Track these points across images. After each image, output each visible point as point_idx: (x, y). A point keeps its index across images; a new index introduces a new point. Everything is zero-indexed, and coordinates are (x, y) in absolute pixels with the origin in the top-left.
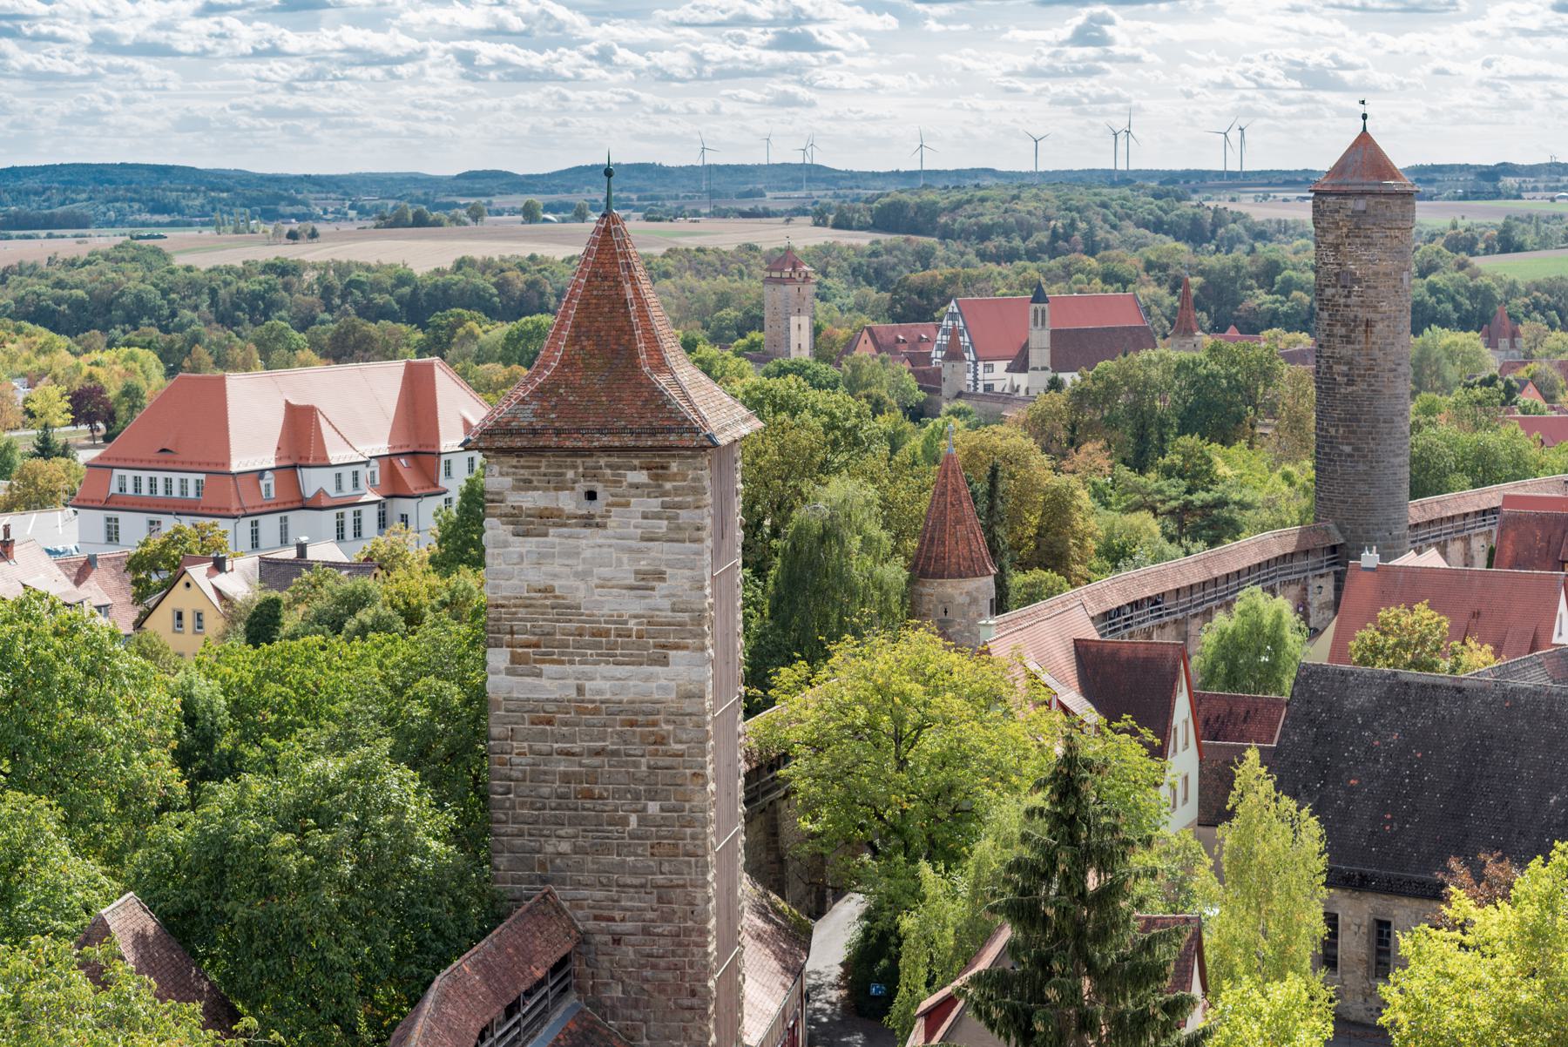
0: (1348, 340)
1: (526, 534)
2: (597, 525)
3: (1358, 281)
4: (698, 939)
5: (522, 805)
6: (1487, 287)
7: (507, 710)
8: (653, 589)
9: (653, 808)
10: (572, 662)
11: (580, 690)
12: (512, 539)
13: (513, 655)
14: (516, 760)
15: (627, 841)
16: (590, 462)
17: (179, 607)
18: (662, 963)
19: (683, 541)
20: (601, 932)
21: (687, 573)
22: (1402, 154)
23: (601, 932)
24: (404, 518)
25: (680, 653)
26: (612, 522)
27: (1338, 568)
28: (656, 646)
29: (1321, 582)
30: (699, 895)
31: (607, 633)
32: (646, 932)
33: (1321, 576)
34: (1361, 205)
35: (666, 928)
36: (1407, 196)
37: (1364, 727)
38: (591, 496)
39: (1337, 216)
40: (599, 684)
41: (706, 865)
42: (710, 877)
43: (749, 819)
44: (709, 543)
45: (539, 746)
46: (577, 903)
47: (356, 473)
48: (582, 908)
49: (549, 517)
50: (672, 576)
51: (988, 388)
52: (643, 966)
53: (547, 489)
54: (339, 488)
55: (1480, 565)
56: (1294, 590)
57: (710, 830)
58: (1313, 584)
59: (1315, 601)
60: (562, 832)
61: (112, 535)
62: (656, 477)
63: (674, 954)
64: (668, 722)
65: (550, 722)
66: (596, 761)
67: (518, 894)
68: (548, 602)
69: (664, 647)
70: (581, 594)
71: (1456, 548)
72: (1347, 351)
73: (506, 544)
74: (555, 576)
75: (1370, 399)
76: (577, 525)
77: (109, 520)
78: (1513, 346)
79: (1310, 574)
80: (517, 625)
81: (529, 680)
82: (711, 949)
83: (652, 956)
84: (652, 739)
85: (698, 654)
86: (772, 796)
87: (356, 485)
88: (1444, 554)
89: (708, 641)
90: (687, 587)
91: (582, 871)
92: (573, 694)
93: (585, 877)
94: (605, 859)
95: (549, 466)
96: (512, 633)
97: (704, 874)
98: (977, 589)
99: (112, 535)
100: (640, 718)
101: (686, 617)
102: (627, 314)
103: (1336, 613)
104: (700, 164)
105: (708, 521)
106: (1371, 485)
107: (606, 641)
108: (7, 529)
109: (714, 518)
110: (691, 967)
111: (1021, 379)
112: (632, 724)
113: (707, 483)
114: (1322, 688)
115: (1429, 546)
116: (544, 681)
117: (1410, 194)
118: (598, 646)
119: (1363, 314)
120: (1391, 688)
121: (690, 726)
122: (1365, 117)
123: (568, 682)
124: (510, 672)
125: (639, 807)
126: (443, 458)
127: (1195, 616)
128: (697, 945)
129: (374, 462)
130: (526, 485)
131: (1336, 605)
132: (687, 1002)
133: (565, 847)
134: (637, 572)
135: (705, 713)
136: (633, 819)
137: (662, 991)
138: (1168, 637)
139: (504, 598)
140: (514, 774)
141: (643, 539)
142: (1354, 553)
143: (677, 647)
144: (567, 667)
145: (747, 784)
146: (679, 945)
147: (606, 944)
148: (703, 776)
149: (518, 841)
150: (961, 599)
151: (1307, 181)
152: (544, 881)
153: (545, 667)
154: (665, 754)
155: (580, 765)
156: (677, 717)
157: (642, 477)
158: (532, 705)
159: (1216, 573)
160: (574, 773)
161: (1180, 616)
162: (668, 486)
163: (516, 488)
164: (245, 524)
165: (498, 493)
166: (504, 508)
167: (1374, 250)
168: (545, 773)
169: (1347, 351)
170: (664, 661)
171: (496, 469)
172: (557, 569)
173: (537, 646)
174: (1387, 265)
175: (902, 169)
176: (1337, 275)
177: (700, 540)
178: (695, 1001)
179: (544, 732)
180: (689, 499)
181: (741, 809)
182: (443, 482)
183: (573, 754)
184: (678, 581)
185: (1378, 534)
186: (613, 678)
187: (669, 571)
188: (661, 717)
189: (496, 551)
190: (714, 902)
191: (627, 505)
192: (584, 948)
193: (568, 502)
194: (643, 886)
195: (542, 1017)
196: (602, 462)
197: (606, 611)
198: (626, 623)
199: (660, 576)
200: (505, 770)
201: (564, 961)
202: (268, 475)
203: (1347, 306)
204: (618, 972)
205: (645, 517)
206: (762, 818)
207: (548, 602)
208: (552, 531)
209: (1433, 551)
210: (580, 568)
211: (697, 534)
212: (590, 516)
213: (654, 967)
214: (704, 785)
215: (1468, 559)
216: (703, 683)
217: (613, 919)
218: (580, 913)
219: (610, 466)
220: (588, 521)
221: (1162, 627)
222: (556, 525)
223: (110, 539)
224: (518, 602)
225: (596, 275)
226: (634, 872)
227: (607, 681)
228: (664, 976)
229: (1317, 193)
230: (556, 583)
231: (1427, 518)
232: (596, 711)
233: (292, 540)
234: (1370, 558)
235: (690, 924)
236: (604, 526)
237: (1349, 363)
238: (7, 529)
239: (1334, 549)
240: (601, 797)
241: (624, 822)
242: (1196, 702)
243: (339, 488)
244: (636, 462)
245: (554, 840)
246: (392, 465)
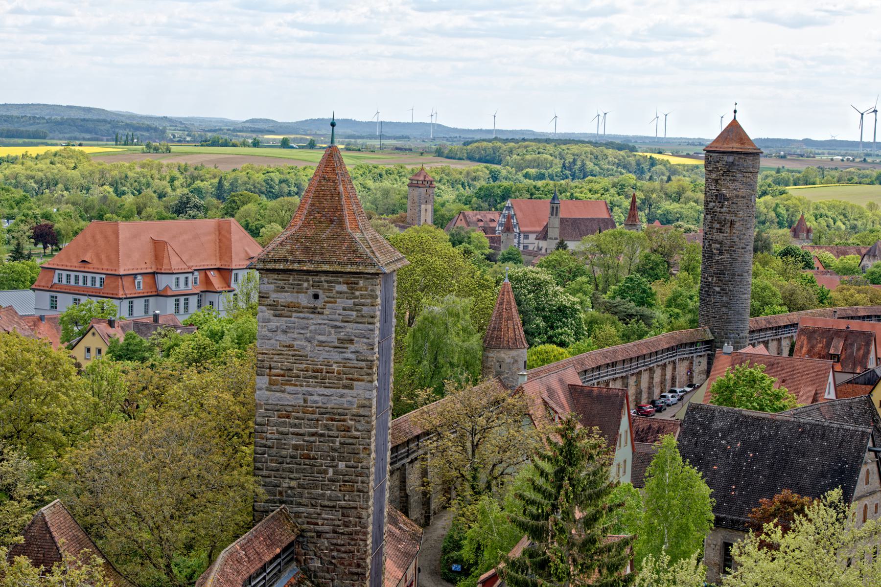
0: (720, 231)
1: (280, 316)
2: (319, 313)
3: (727, 199)
4: (363, 537)
5: (272, 461)
6: (795, 206)
7: (266, 410)
8: (347, 348)
9: (342, 465)
10: (301, 386)
11: (305, 401)
12: (272, 318)
13: (270, 380)
14: (269, 436)
15: (327, 482)
16: (316, 278)
17: (88, 345)
18: (343, 549)
19: (364, 323)
20: (311, 531)
21: (365, 340)
22: (754, 132)
23: (311, 531)
24: (211, 303)
25: (360, 383)
26: (326, 312)
27: (710, 352)
28: (347, 379)
29: (700, 359)
30: (364, 513)
31: (321, 371)
32: (335, 532)
33: (701, 356)
34: (731, 159)
35: (346, 529)
36: (756, 154)
37: (722, 438)
38: (316, 297)
39: (718, 165)
40: (316, 398)
41: (368, 497)
42: (370, 503)
43: (392, 473)
44: (378, 325)
45: (281, 429)
46: (298, 515)
48: (301, 517)
49: (293, 307)
50: (357, 342)
51: (525, 247)
52: (332, 550)
53: (293, 292)
54: (177, 285)
55: (786, 353)
56: (686, 363)
57: (371, 478)
58: (696, 361)
59: (697, 369)
60: (292, 476)
61: (54, 306)
62: (352, 289)
63: (349, 544)
64: (351, 420)
65: (288, 417)
66: (312, 439)
67: (267, 508)
68: (290, 353)
69: (351, 379)
70: (308, 349)
71: (773, 345)
72: (720, 237)
73: (269, 321)
74: (295, 339)
75: (731, 263)
76: (308, 312)
77: (52, 297)
78: (807, 237)
79: (695, 355)
80: (273, 364)
81: (278, 394)
82: (368, 543)
83: (337, 545)
84: (342, 428)
85: (369, 384)
86: (403, 461)
87: (186, 284)
88: (767, 347)
89: (375, 377)
90: (365, 348)
91: (302, 497)
92: (301, 402)
93: (304, 501)
94: (313, 491)
95: (294, 280)
96: (270, 368)
97: (367, 502)
98: (518, 356)
99: (54, 306)
100: (337, 417)
101: (363, 364)
102: (340, 200)
103: (708, 376)
104: (375, 120)
105: (378, 313)
106: (730, 309)
107: (319, 375)
109: (381, 311)
110: (358, 551)
111: (543, 244)
112: (332, 420)
113: (378, 293)
114: (700, 417)
115: (759, 343)
116: (286, 395)
117: (758, 154)
118: (316, 377)
119: (729, 217)
120: (737, 419)
121: (363, 422)
122: (735, 112)
123: (300, 396)
124: (268, 389)
125: (334, 464)
126: (234, 272)
127: (633, 374)
128: (362, 540)
129: (196, 273)
130: (282, 289)
131: (708, 372)
132: (354, 570)
133: (293, 484)
134: (339, 339)
135: (371, 416)
136: (331, 471)
137: (343, 564)
138: (618, 385)
139: (267, 350)
140: (269, 443)
141: (343, 321)
142: (718, 345)
143: (358, 380)
144: (299, 389)
145: (392, 453)
146: (352, 539)
147: (313, 537)
148: (370, 449)
149: (268, 480)
150: (508, 361)
151: (700, 144)
152: (282, 502)
153: (287, 387)
154: (350, 437)
155: (304, 441)
156: (357, 417)
157: (344, 288)
158: (279, 407)
159: (645, 352)
160: (300, 445)
161: (624, 374)
162: (357, 293)
163: (275, 291)
164: (126, 304)
166: (268, 301)
167: (736, 183)
168: (285, 444)
169: (720, 237)
170: (350, 387)
171: (266, 280)
172: (296, 336)
173: (283, 376)
174: (743, 192)
175: (484, 129)
176: (716, 196)
177: (373, 323)
178: (360, 570)
179: (285, 423)
180: (369, 301)
181: (389, 468)
182: (233, 285)
183: (301, 435)
184: (360, 345)
185: (732, 336)
186: (323, 395)
187: (356, 339)
188: (348, 417)
190: (371, 517)
191: (335, 302)
192: (301, 539)
193: (304, 300)
194: (334, 507)
195: (277, 576)
196: (323, 279)
197: (321, 359)
198: (331, 366)
199: (351, 341)
200: (264, 441)
201: (291, 545)
202: (139, 277)
203: (721, 213)
204: (319, 553)
205: (344, 309)
206: (398, 473)
207: (290, 353)
208: (294, 314)
209: (762, 346)
210: (308, 335)
211: (371, 320)
212: (315, 308)
213: (339, 551)
214: (369, 455)
215: (780, 352)
216: (370, 399)
217: (317, 524)
218: (300, 520)
219: (327, 282)
220: (314, 310)
221: (615, 380)
222: (296, 311)
223: (52, 307)
224: (274, 352)
225: (325, 179)
226: (330, 499)
227: (318, 396)
228: (343, 555)
229: (708, 151)
230: (295, 343)
231: (759, 327)
232: (313, 413)
233: (151, 313)
234: (728, 348)
235: (358, 528)
236: (322, 313)
237: (721, 243)
239: (707, 342)
240: (315, 459)
241: (325, 472)
242: (631, 422)
243: (177, 285)
244: (341, 280)
245: (287, 480)
246: (206, 276)
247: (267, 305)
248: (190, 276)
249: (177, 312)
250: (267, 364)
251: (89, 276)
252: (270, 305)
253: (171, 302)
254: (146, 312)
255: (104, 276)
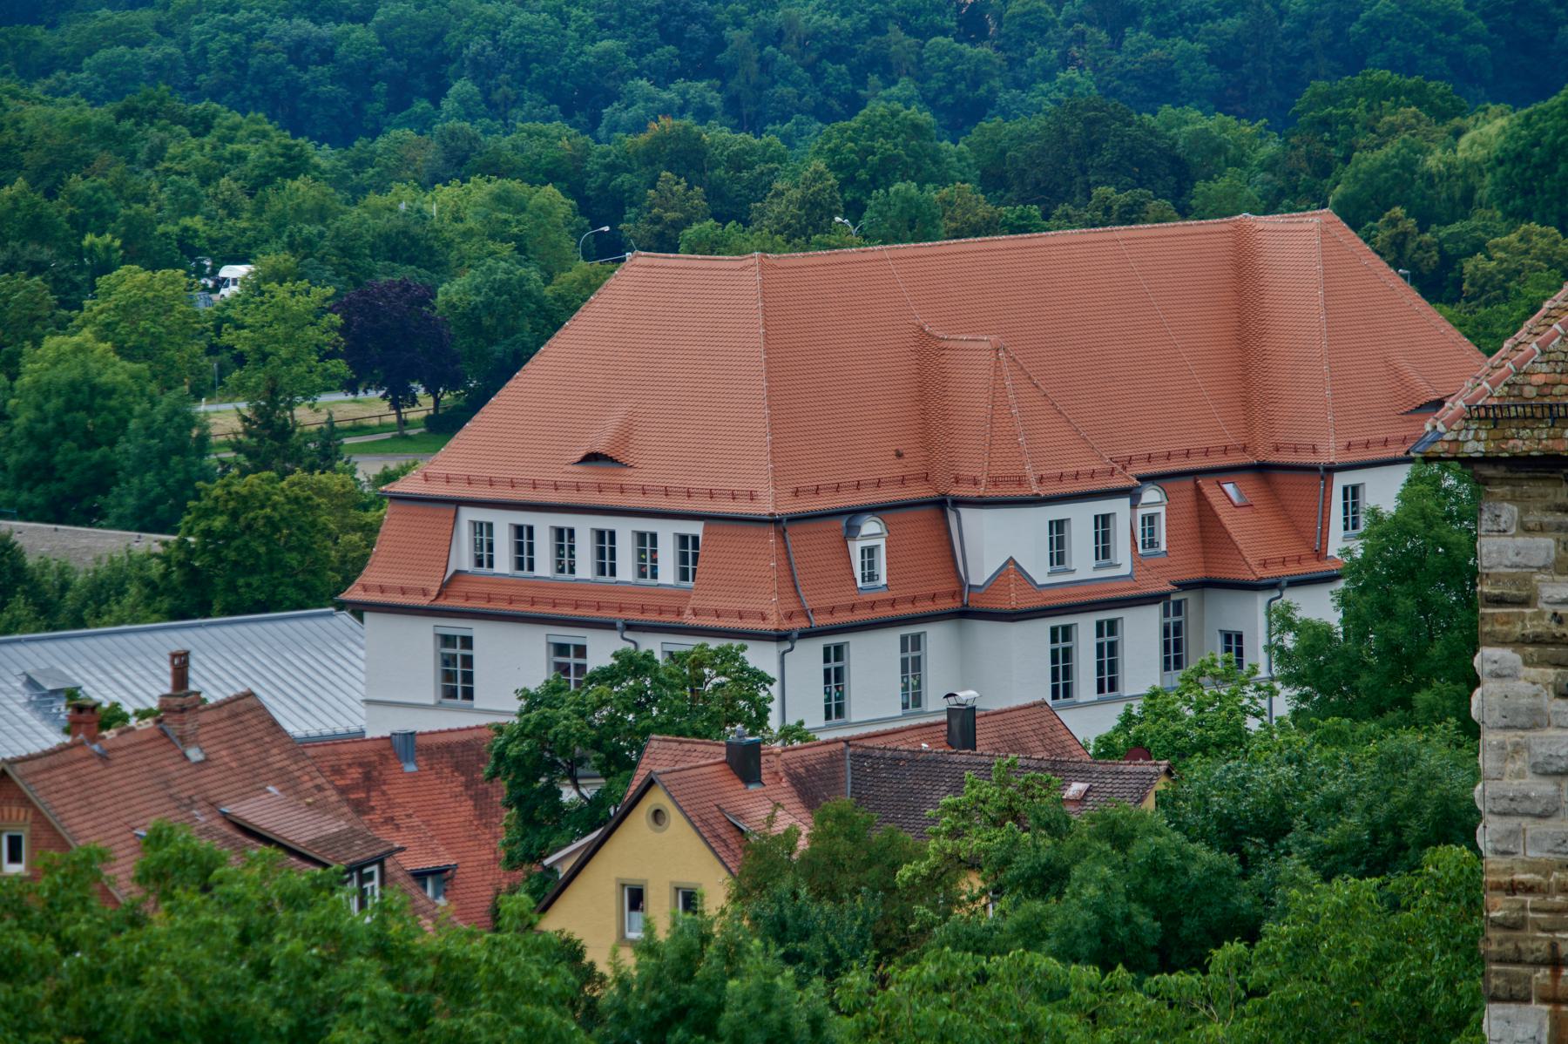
17: (633, 875)
47: (1103, 521)
54: (1058, 557)
61: (457, 679)
73: (1536, 720)
77: (447, 640)
87: (1103, 550)
99: (457, 679)
108: (181, 666)
129: (1151, 495)
139: (1533, 867)
165: (1514, 580)
166: (1531, 622)
189: (1511, 737)
202: (871, 526)
223: (450, 693)
238: (181, 666)
243: (1058, 557)
247: (1521, 642)
248: (1119, 508)
249: (1062, 685)
250: (1538, 943)
251: (625, 530)
252: (1537, 641)
253: (1034, 638)
254: (913, 697)
255: (695, 528)
